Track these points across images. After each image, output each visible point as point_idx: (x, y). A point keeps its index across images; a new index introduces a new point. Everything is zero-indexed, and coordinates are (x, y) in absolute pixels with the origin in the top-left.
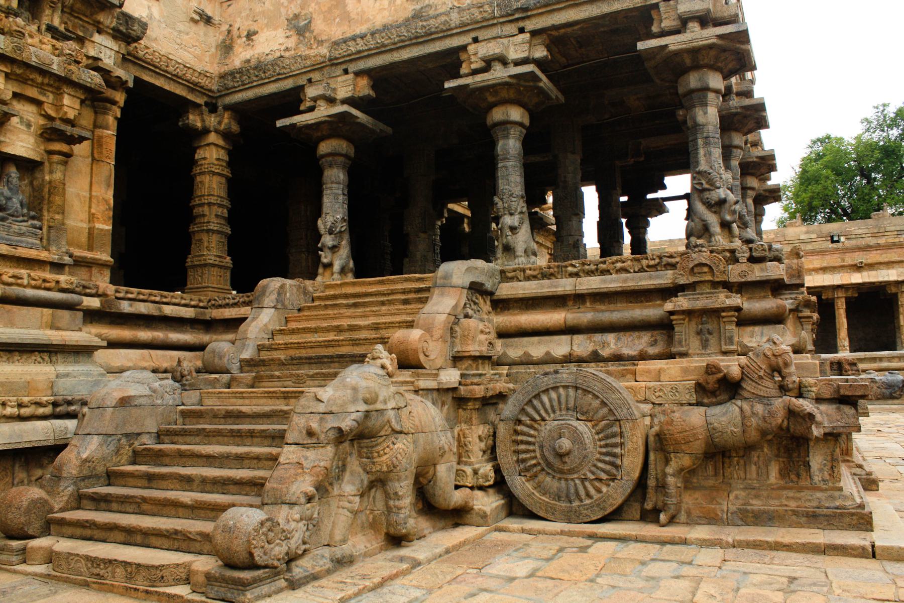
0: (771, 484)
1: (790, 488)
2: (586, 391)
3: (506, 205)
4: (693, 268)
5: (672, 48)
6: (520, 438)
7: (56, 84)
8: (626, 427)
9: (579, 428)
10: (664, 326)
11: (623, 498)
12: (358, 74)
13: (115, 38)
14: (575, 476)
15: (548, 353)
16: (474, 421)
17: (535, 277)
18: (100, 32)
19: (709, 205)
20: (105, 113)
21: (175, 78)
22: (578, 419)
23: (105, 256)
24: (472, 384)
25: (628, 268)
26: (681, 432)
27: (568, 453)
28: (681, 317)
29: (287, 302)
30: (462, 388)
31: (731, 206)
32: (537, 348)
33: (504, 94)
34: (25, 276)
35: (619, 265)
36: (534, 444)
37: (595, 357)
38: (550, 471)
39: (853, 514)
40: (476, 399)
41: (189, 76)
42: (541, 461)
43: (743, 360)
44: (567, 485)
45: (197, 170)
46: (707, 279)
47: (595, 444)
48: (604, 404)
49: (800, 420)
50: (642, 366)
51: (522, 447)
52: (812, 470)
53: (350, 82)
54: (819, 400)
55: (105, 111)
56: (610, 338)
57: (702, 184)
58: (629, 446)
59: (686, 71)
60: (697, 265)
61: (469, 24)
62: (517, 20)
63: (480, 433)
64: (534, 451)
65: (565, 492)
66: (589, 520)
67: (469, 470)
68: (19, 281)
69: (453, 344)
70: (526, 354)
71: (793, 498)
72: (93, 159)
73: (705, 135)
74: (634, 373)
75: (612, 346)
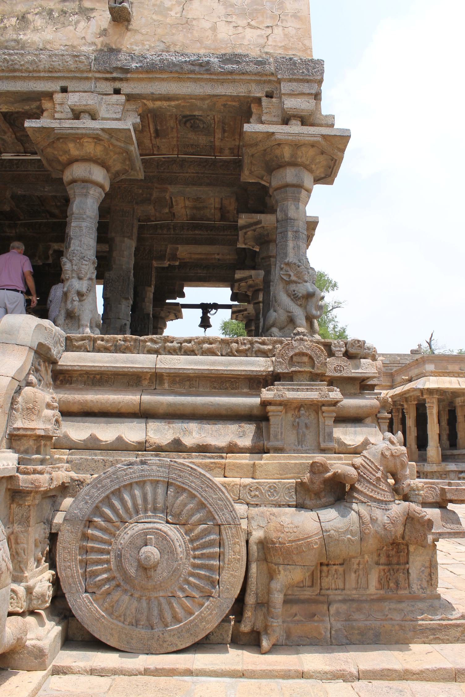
0: (371, 595)
2: (181, 490)
3: (75, 268)
4: (292, 357)
5: (278, 136)
8: (227, 533)
9: (169, 533)
10: (259, 418)
11: (220, 620)
14: (161, 594)
15: (120, 439)
16: (32, 522)
17: (106, 350)
19: (294, 297)
22: (168, 522)
24: (35, 472)
25: (216, 350)
26: (294, 541)
27: (155, 567)
28: (280, 408)
30: (21, 476)
31: (318, 301)
32: (107, 432)
33: (90, 148)
36: (108, 553)
37: (177, 446)
38: (128, 587)
39: (458, 626)
40: (37, 492)
42: (117, 575)
43: (358, 460)
44: (148, 604)
46: (307, 369)
47: (188, 554)
48: (202, 506)
49: (418, 527)
50: (231, 459)
51: (94, 556)
52: (411, 578)
54: (425, 504)
56: (193, 426)
57: (290, 276)
58: (229, 555)
59: (281, 165)
60: (296, 355)
61: (60, 71)
62: (114, 79)
63: (37, 536)
64: (108, 562)
65: (145, 614)
66: (175, 649)
67: (20, 589)
69: (10, 418)
70: (93, 438)
71: (395, 609)
73: (295, 229)
75: (194, 434)
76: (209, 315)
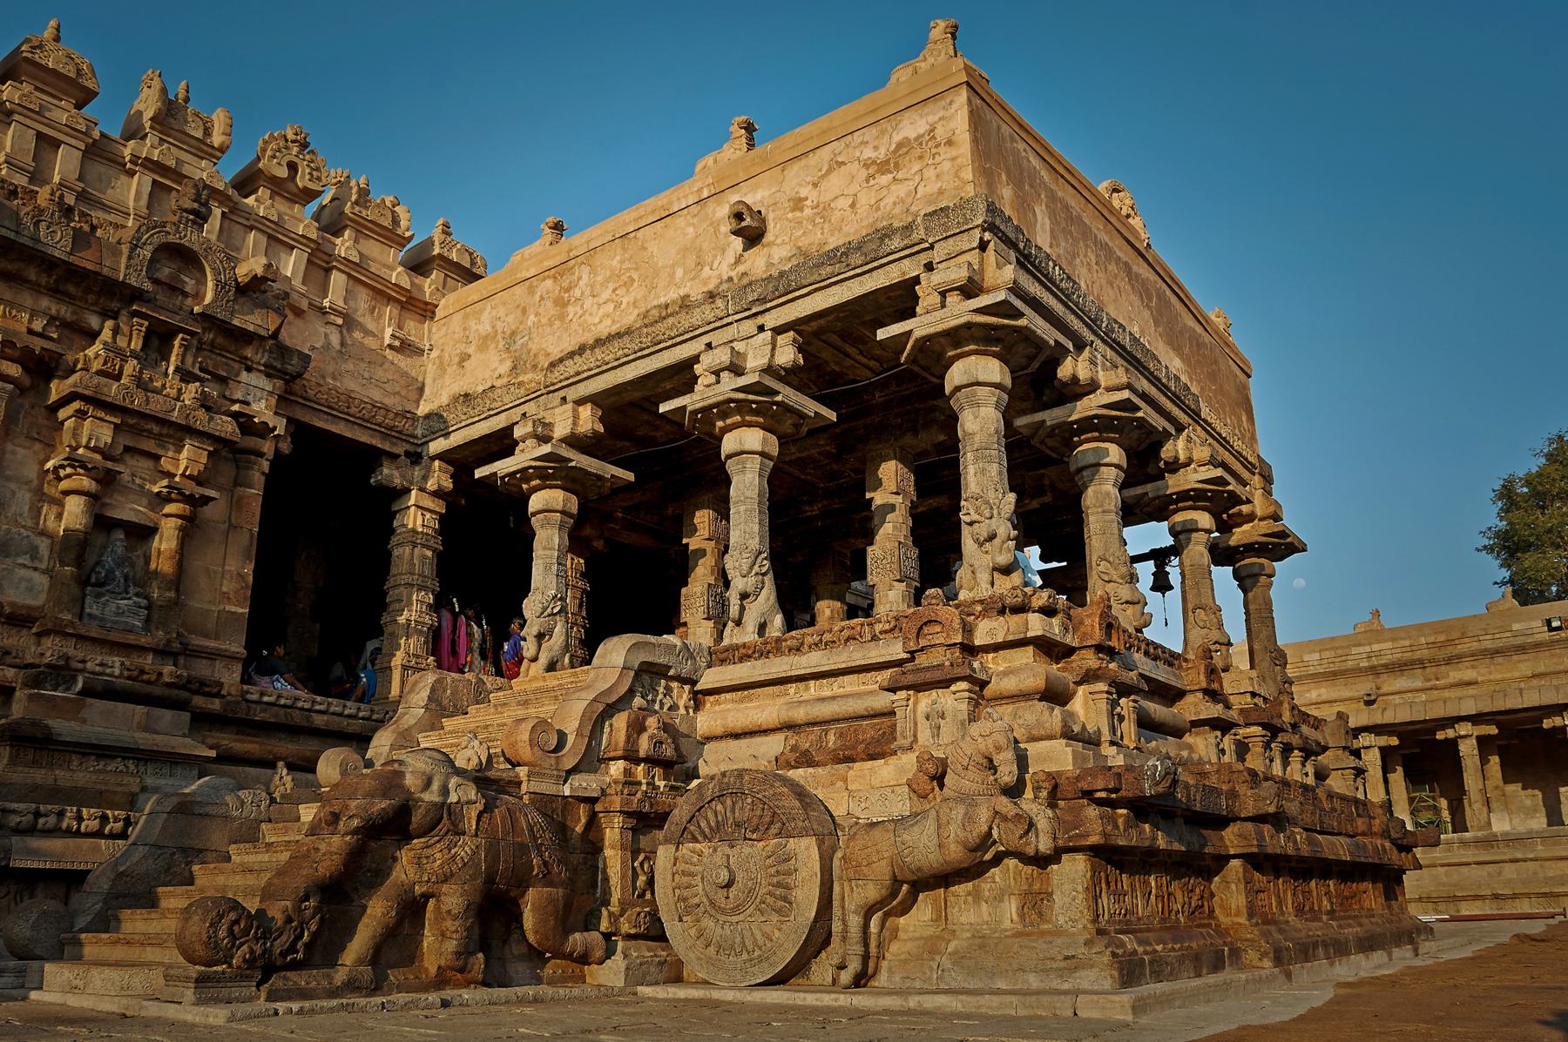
1: (1029, 934)
6: (681, 866)
7: (179, 434)
12: (580, 402)
13: (268, 376)
14: (741, 917)
18: (249, 369)
20: (248, 468)
21: (363, 423)
23: (237, 646)
29: (445, 702)
34: (117, 664)
35: (846, 633)
41: (379, 419)
45: (394, 540)
53: (570, 414)
55: (249, 466)
68: (108, 671)
72: (230, 525)
74: (845, 780)
76: (1168, 569)
